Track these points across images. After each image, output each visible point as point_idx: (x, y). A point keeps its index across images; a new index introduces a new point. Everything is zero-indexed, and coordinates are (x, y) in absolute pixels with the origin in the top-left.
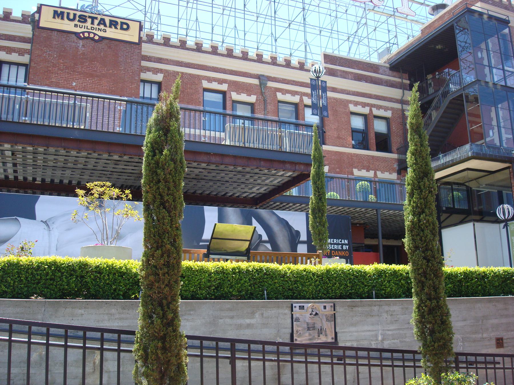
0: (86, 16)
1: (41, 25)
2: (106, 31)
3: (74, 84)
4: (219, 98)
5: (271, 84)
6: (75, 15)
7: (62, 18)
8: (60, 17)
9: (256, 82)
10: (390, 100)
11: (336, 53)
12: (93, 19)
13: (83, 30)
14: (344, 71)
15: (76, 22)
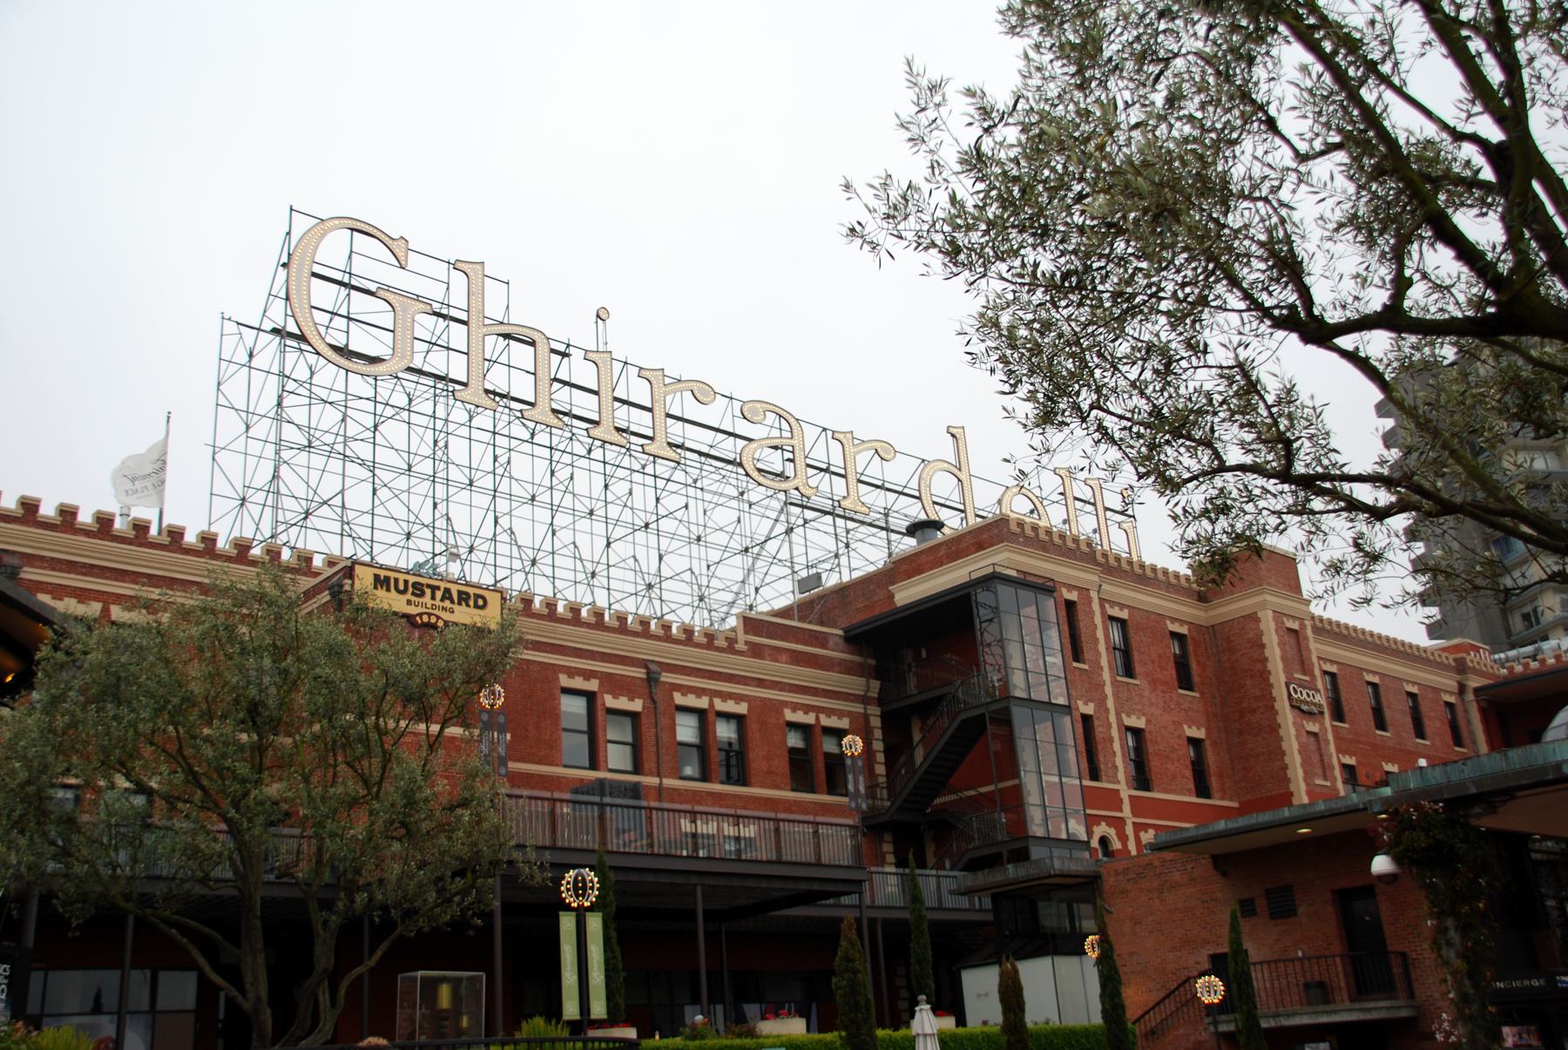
5: (667, 678)
6: (406, 582)
7: (388, 590)
9: (639, 673)
12: (434, 588)
13: (419, 610)
15: (409, 596)
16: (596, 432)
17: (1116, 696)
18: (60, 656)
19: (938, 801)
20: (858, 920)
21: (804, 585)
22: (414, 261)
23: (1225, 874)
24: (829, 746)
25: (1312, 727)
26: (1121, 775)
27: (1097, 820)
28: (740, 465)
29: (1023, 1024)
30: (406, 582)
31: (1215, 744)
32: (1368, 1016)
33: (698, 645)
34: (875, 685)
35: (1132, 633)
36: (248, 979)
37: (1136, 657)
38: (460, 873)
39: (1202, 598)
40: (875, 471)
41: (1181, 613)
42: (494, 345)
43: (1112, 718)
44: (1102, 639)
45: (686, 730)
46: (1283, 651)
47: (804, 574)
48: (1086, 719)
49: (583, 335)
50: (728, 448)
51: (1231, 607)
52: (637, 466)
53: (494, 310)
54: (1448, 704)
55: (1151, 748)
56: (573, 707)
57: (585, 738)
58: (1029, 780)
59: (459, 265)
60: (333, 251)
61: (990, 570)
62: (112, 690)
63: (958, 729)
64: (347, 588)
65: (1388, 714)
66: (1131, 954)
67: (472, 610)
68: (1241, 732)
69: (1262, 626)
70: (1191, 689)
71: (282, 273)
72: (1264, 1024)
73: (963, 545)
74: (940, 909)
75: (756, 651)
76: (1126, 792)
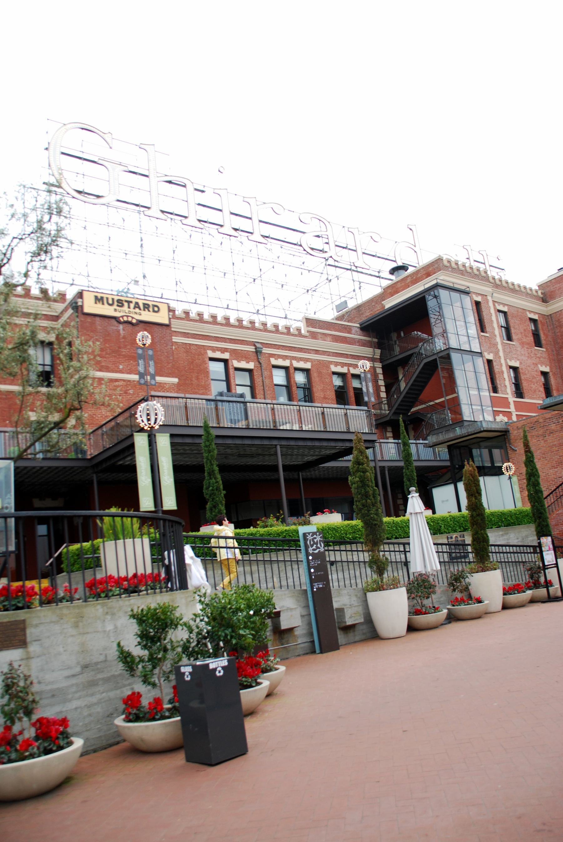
0: (122, 301)
1: (86, 310)
2: (140, 315)
3: (121, 367)
4: (220, 366)
6: (113, 299)
7: (103, 304)
8: (101, 303)
9: (252, 349)
11: (316, 317)
12: (129, 302)
14: (324, 334)
15: (115, 307)
17: (504, 351)
19: (413, 410)
20: (375, 467)
24: (355, 384)
28: (301, 246)
30: (113, 299)
31: (554, 374)
33: (282, 333)
34: (378, 351)
35: (510, 318)
37: (513, 331)
39: (544, 300)
41: (535, 309)
43: (503, 361)
44: (495, 322)
45: (279, 378)
48: (489, 362)
55: (523, 377)
56: (217, 369)
57: (225, 383)
59: (142, 146)
61: (434, 282)
63: (423, 368)
64: (80, 304)
67: (152, 313)
70: (541, 347)
73: (419, 275)
75: (314, 335)
76: (512, 399)
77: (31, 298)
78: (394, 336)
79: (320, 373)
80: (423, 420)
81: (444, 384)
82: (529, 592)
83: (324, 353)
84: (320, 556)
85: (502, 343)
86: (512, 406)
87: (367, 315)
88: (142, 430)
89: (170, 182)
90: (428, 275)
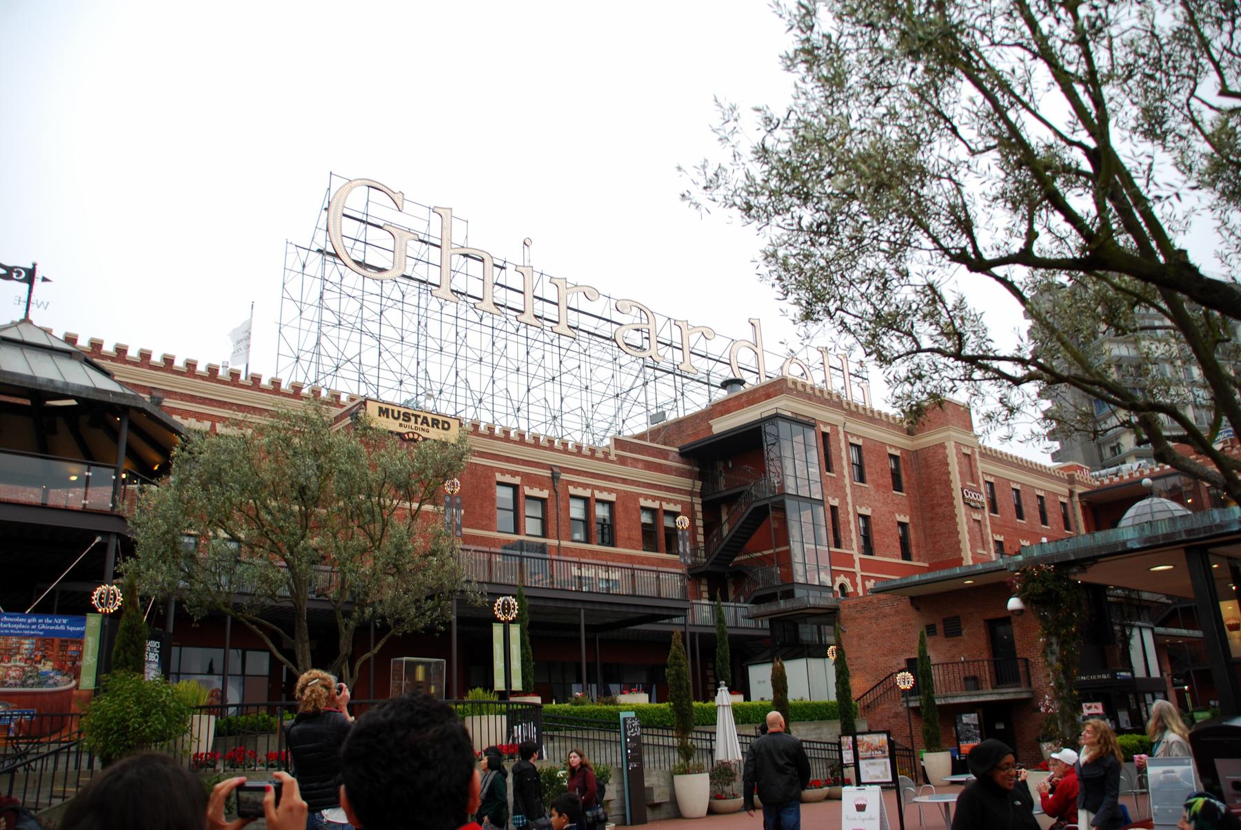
5: (564, 476)
9: (547, 473)
10: (680, 491)
12: (417, 416)
14: (634, 459)
15: (400, 421)
16: (521, 318)
18: (186, 454)
19: (737, 559)
20: (684, 634)
21: (653, 419)
22: (407, 207)
23: (918, 609)
24: (668, 522)
25: (977, 516)
26: (855, 545)
27: (839, 573)
28: (615, 340)
29: (786, 700)
31: (915, 526)
32: (1002, 698)
33: (585, 456)
34: (699, 484)
35: (864, 453)
36: (299, 658)
37: (867, 470)
38: (431, 597)
39: (910, 432)
40: (701, 347)
41: (897, 442)
42: (458, 261)
43: (850, 509)
44: (845, 458)
45: (576, 510)
46: (960, 468)
47: (654, 412)
48: (834, 509)
49: (514, 256)
50: (606, 329)
51: (927, 439)
52: (548, 340)
53: (458, 239)
54: (1062, 503)
55: (874, 528)
56: (504, 494)
58: (795, 547)
60: (356, 201)
61: (774, 412)
62: (215, 477)
65: (1024, 508)
66: (857, 658)
67: (441, 431)
68: (932, 519)
69: (947, 451)
70: (901, 491)
71: (325, 213)
72: (938, 702)
74: (736, 627)
75: (622, 461)
76: (857, 556)
77: (301, 398)
78: (720, 465)
79: (626, 508)
80: (746, 576)
81: (775, 530)
82: (826, 788)
83: (633, 483)
84: (636, 739)
85: (852, 485)
86: (857, 565)
87: (688, 440)
88: (499, 621)
89: (466, 255)
90: (768, 396)
